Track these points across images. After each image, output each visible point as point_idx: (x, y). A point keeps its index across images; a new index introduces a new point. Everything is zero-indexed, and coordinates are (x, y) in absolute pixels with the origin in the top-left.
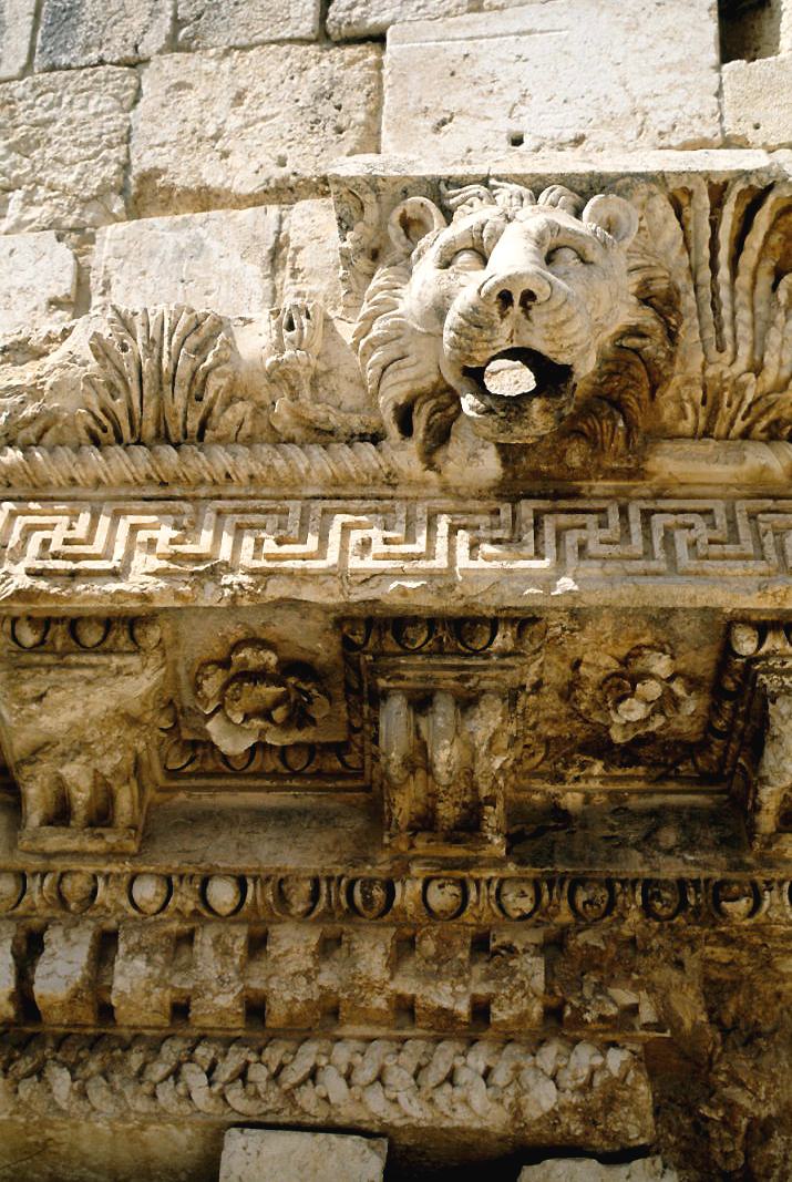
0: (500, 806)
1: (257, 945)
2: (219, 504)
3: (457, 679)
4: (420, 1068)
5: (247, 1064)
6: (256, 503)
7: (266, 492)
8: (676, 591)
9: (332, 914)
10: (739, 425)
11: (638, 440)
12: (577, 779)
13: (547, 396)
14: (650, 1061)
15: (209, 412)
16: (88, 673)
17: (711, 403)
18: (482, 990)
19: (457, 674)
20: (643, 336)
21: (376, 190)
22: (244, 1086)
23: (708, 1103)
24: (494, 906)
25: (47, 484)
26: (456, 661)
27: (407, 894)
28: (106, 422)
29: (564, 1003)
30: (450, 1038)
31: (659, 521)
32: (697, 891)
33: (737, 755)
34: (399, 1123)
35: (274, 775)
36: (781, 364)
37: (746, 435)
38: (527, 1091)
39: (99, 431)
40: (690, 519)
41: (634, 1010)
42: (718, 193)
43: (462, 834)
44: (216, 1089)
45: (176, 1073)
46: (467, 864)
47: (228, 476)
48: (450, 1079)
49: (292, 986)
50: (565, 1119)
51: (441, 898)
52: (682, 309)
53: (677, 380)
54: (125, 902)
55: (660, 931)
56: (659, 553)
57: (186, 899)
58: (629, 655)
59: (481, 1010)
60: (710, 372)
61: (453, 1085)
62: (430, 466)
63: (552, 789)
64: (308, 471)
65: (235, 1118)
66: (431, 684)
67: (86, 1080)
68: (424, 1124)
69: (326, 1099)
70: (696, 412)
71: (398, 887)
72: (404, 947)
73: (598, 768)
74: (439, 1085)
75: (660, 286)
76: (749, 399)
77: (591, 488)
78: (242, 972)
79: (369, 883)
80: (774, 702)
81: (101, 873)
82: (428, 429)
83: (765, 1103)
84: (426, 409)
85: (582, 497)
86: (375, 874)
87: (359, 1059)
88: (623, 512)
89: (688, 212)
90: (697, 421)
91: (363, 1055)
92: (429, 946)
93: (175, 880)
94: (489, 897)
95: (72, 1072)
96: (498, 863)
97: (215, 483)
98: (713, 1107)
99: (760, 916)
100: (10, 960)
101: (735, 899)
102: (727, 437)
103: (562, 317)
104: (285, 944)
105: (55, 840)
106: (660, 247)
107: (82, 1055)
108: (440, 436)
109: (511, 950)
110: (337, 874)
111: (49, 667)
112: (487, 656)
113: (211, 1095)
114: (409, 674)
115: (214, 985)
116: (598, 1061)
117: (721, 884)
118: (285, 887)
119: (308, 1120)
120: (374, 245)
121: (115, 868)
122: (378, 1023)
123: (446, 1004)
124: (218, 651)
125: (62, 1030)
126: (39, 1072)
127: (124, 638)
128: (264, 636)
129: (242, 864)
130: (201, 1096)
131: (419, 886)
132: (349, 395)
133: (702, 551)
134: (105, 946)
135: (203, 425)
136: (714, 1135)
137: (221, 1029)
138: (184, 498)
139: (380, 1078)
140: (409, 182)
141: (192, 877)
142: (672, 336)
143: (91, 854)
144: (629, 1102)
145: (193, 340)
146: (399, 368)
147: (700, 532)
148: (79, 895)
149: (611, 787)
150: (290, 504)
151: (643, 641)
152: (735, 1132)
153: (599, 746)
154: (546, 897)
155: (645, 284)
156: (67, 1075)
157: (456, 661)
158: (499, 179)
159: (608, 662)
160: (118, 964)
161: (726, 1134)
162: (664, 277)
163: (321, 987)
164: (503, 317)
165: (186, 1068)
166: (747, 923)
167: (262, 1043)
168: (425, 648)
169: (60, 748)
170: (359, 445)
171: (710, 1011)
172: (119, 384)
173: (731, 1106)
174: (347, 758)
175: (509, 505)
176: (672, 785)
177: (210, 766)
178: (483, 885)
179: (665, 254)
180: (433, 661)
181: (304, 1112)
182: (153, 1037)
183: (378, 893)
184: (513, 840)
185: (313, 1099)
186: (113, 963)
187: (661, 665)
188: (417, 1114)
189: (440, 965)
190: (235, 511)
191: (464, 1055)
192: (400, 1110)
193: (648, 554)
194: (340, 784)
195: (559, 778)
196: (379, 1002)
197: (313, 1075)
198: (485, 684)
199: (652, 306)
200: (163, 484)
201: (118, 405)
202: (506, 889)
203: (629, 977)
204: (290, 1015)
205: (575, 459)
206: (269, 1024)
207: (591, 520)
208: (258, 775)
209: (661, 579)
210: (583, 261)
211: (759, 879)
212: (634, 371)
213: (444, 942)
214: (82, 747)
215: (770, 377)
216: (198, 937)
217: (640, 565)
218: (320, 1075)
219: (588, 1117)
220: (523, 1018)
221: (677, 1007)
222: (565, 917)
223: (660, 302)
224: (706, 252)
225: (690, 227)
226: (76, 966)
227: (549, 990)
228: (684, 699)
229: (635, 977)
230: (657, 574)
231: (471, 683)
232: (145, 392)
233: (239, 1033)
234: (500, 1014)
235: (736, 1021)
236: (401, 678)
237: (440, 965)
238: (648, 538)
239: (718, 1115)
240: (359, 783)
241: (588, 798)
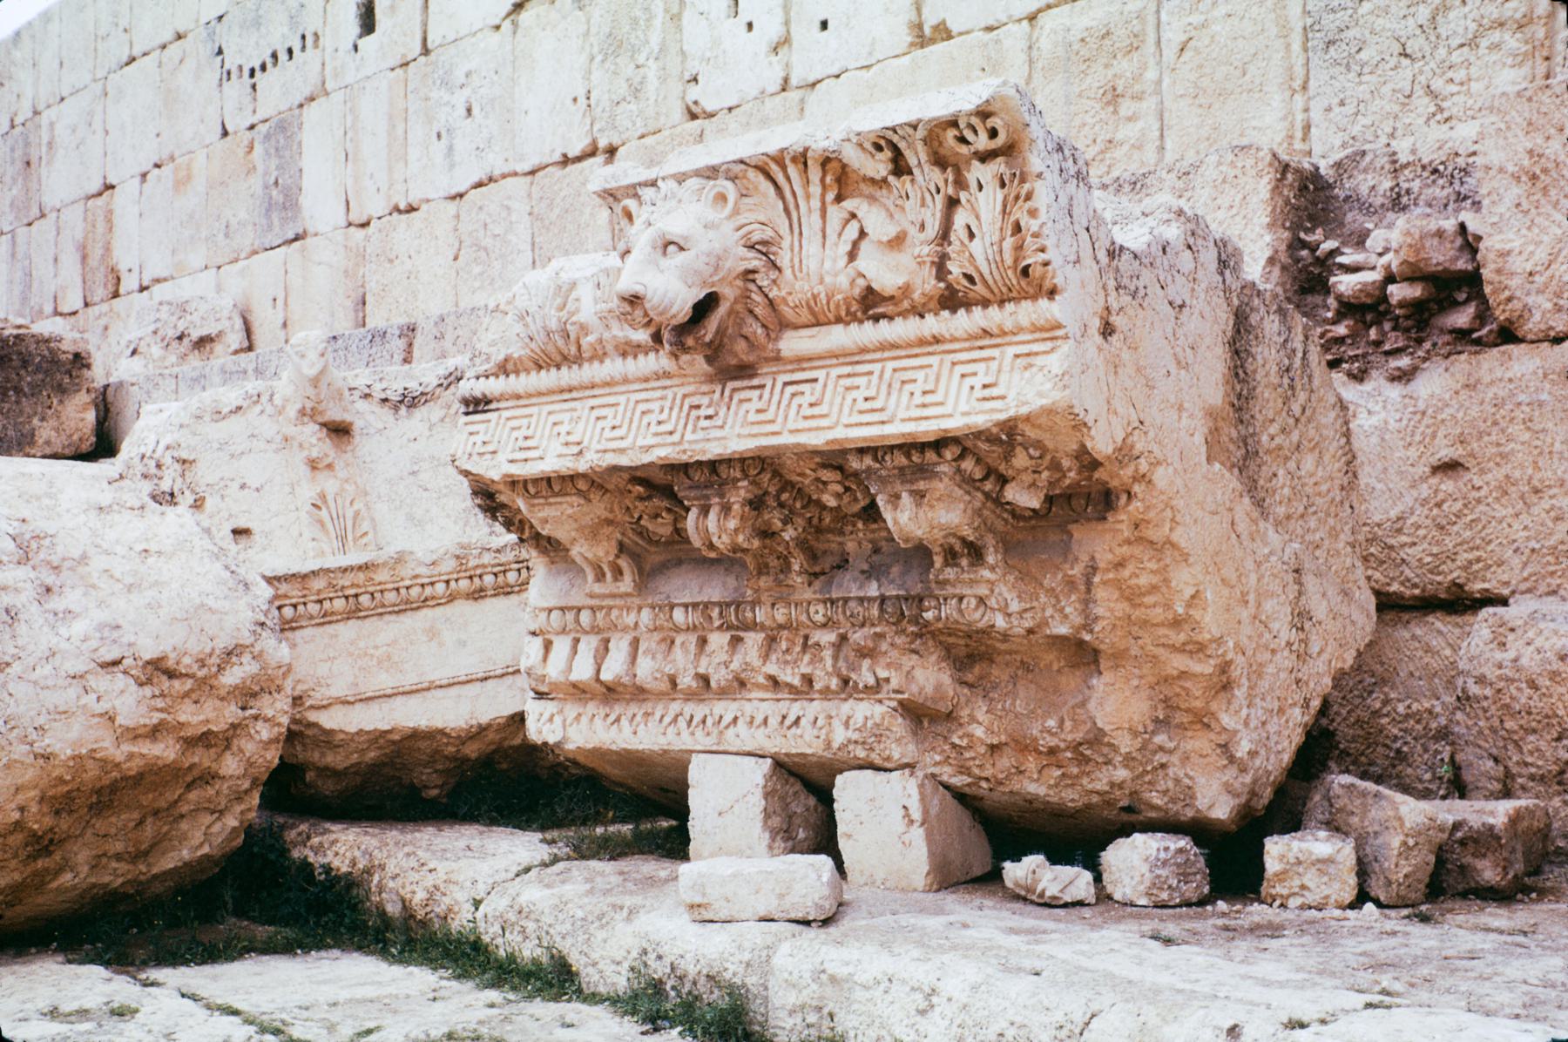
18: (806, 670)
41: (887, 680)
59: (808, 680)
73: (860, 525)
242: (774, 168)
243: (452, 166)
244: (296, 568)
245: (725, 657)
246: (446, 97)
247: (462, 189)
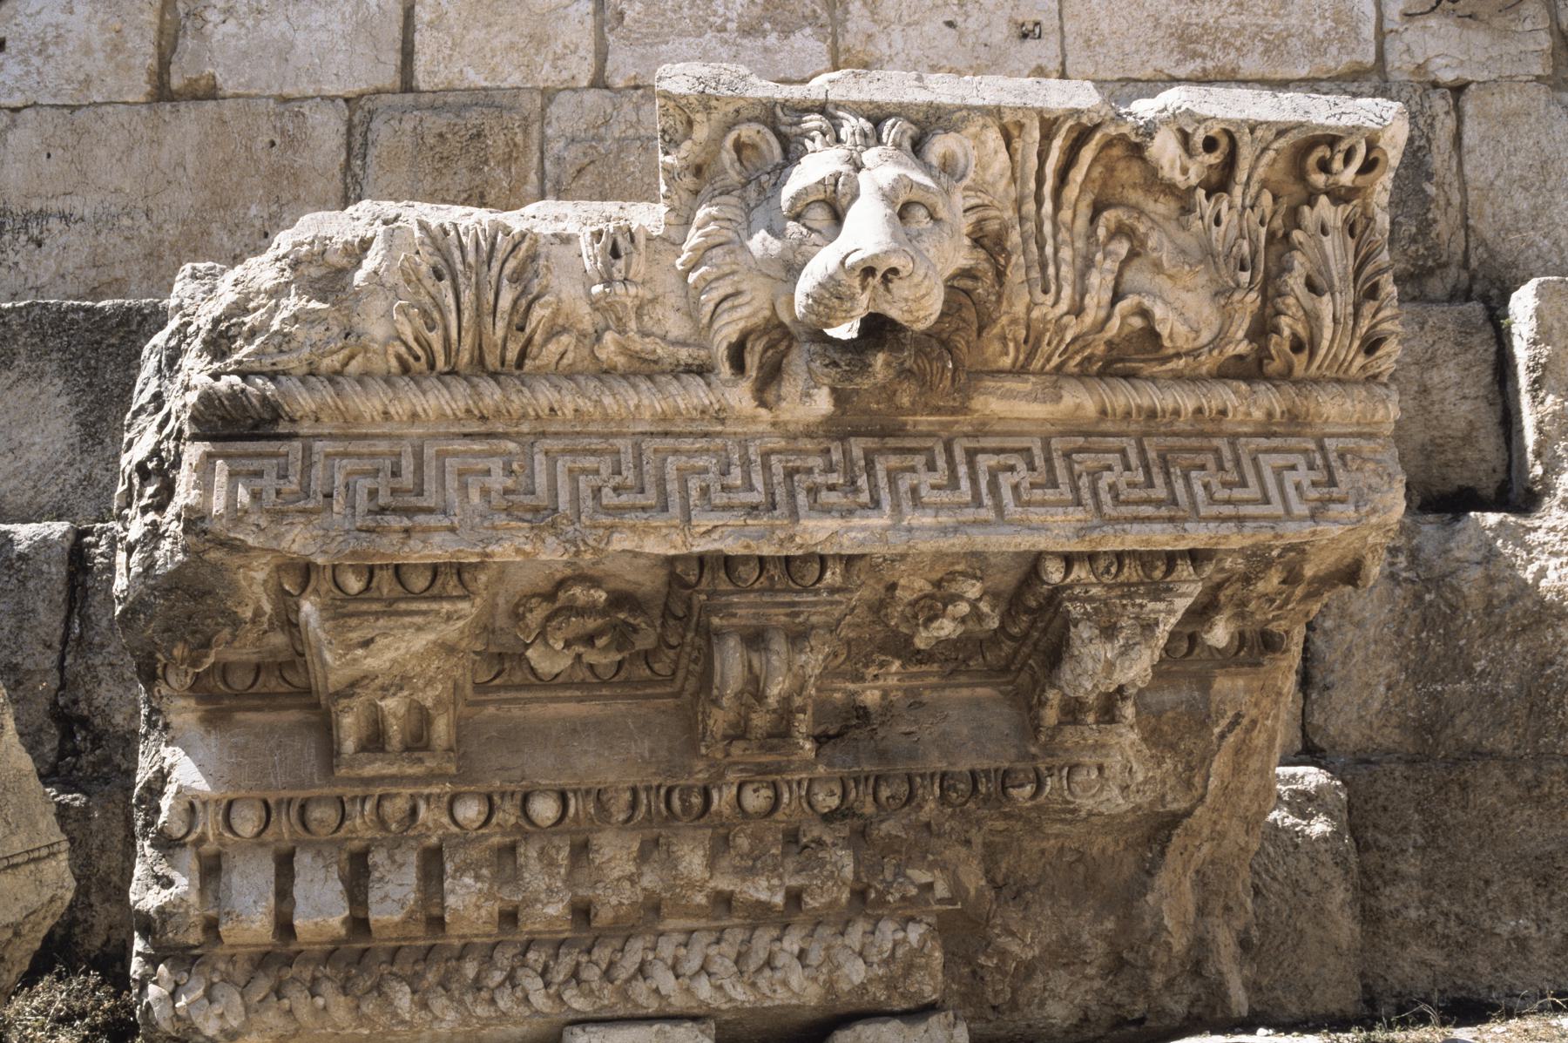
0: (810, 712)
1: (581, 851)
2: (548, 443)
3: (787, 615)
4: (740, 954)
5: (578, 964)
6: (583, 442)
7: (592, 428)
8: (1003, 539)
9: (651, 821)
10: (1056, 360)
11: (963, 377)
12: (876, 677)
13: (891, 350)
14: (944, 928)
15: (529, 341)
16: (419, 620)
17: (1032, 342)
18: (794, 882)
19: (789, 610)
20: (975, 278)
21: (708, 109)
22: (578, 984)
23: (985, 953)
24: (805, 805)
25: (358, 418)
26: (787, 598)
27: (722, 800)
28: (420, 352)
29: (869, 886)
30: (765, 925)
31: (985, 462)
32: (989, 781)
33: (1029, 656)
34: (724, 1007)
35: (582, 684)
36: (1099, 306)
37: (1059, 369)
38: (838, 967)
39: (411, 360)
40: (1012, 460)
42: (1049, 127)
43: (775, 741)
44: (552, 991)
45: (511, 979)
47: (552, 409)
48: (769, 963)
49: (617, 890)
50: (871, 989)
51: (755, 800)
52: (1009, 245)
53: (1004, 320)
54: (445, 820)
55: (952, 816)
56: (987, 500)
57: (508, 814)
58: (942, 579)
59: (795, 897)
60: (1035, 314)
61: (773, 969)
62: (763, 403)
63: (851, 686)
64: (637, 407)
65: (571, 1017)
66: (763, 621)
67: (427, 991)
68: (747, 1005)
69: (657, 991)
70: (1017, 350)
71: (715, 795)
72: (721, 844)
73: (896, 666)
74: (759, 970)
75: (993, 226)
76: (1068, 339)
77: (915, 424)
78: (570, 881)
79: (686, 792)
80: (1076, 626)
81: (421, 796)
82: (760, 368)
83: (1030, 946)
84: (759, 347)
85: (908, 435)
86: (691, 782)
87: (683, 951)
88: (949, 450)
89: (1017, 144)
90: (1016, 358)
91: (686, 945)
92: (743, 843)
93: (496, 798)
94: (800, 797)
95: (410, 985)
97: (538, 417)
98: (989, 957)
99: (1041, 799)
100: (340, 886)
101: (1021, 786)
102: (1041, 372)
103: (923, 291)
104: (608, 852)
105: (375, 768)
106: (989, 178)
107: (417, 968)
108: (772, 374)
109: (820, 842)
110: (655, 783)
111: (377, 615)
112: (817, 593)
113: (548, 996)
114: (740, 612)
115: (543, 896)
116: (900, 935)
117: (1006, 773)
118: (604, 798)
119: (641, 1012)
120: (698, 161)
121: (435, 790)
122: (697, 916)
123: (764, 896)
124: (544, 586)
125: (393, 944)
126: (378, 987)
127: (453, 581)
128: (591, 572)
129: (563, 781)
130: (539, 1000)
131: (734, 790)
132: (676, 326)
133: (1025, 498)
134: (432, 865)
135: (523, 355)
136: (988, 978)
137: (550, 932)
138: (505, 436)
139: (704, 968)
140: (742, 102)
141: (513, 794)
142: (1000, 275)
143: (409, 777)
144: (926, 967)
145: (511, 264)
146: (734, 308)
147: (1022, 474)
148: (399, 816)
149: (906, 684)
150: (620, 443)
151: (958, 568)
152: (1005, 974)
153: (902, 647)
154: (853, 795)
155: (979, 224)
156: (407, 989)
157: (787, 598)
158: (837, 106)
159: (921, 585)
160: (447, 884)
161: (998, 977)
162: (996, 218)
163: (644, 889)
164: (864, 288)
165: (520, 972)
166: (1028, 804)
167: (589, 942)
168: (757, 586)
169: (378, 682)
170: (684, 377)
171: (987, 872)
172: (436, 315)
173: (1003, 954)
174: (656, 667)
175: (837, 443)
176: (963, 679)
177: (518, 678)
178: (795, 786)
179: (993, 185)
180: (766, 599)
181: (636, 1005)
182: (482, 944)
183: (696, 800)
184: (821, 740)
185: (645, 992)
186: (442, 882)
187: (973, 590)
188: (742, 997)
189: (755, 860)
190: (564, 452)
191: (780, 939)
192: (725, 995)
193: (977, 502)
194: (649, 691)
195: (859, 678)
196: (700, 899)
197: (642, 971)
198: (814, 619)
199: (983, 247)
200: (483, 418)
201: (435, 338)
202: (816, 788)
203: (925, 858)
204: (617, 919)
205: (905, 401)
206: (593, 924)
207: (919, 461)
208: (568, 685)
209: (990, 529)
210: (932, 217)
211: (1042, 767)
212: (965, 313)
213: (756, 838)
214: (400, 683)
215: (1089, 319)
216: (521, 850)
217: (969, 514)
218: (648, 969)
219: (891, 984)
220: (833, 903)
221: (964, 878)
222: (869, 809)
223: (987, 241)
224: (1032, 185)
225: (1018, 157)
226: (407, 889)
227: (856, 873)
228: (988, 616)
229: (930, 857)
230: (986, 523)
231: (801, 619)
232: (464, 324)
233: (566, 935)
234: (811, 903)
235: (1006, 877)
236: (734, 615)
237: (755, 860)
238: (974, 481)
239: (992, 963)
240: (669, 690)
241: (885, 693)
245: (631, 868)
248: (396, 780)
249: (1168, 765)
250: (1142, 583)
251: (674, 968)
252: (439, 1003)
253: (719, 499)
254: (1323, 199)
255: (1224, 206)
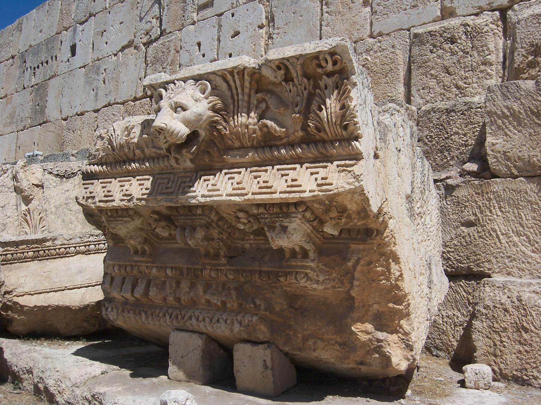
1: (178, 283)
46: (218, 265)
50: (242, 333)
73: (252, 237)
96: (224, 265)
116: (250, 319)
126: (140, 314)
184: (230, 258)
195: (243, 240)
196: (203, 300)
198: (197, 223)
241: (251, 244)
242: (229, 77)
243: (97, 100)
244: (14, 239)
246: (97, 77)
247: (99, 108)
248: (141, 261)
249: (334, 275)
250: (281, 213)
251: (197, 320)
252: (150, 319)
253: (164, 191)
254: (325, 77)
255: (291, 86)
